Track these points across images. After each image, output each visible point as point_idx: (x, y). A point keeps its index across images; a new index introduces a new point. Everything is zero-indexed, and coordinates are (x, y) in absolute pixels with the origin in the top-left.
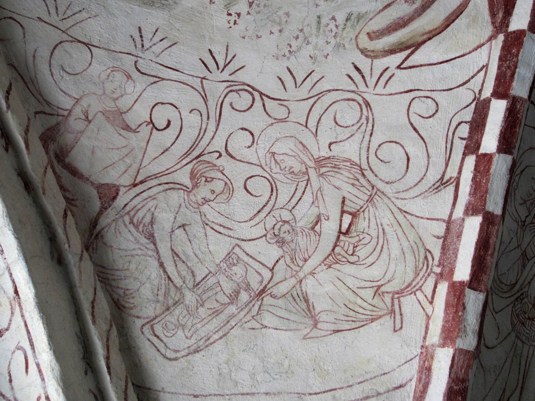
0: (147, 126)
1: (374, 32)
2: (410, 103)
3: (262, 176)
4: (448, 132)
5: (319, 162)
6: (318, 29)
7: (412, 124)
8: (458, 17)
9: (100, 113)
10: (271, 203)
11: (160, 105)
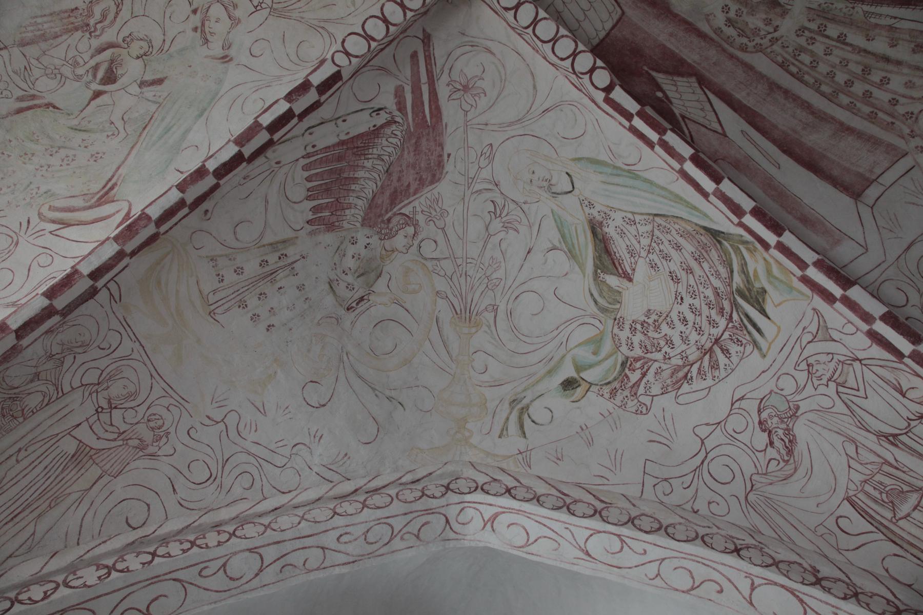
6: (25, 189)
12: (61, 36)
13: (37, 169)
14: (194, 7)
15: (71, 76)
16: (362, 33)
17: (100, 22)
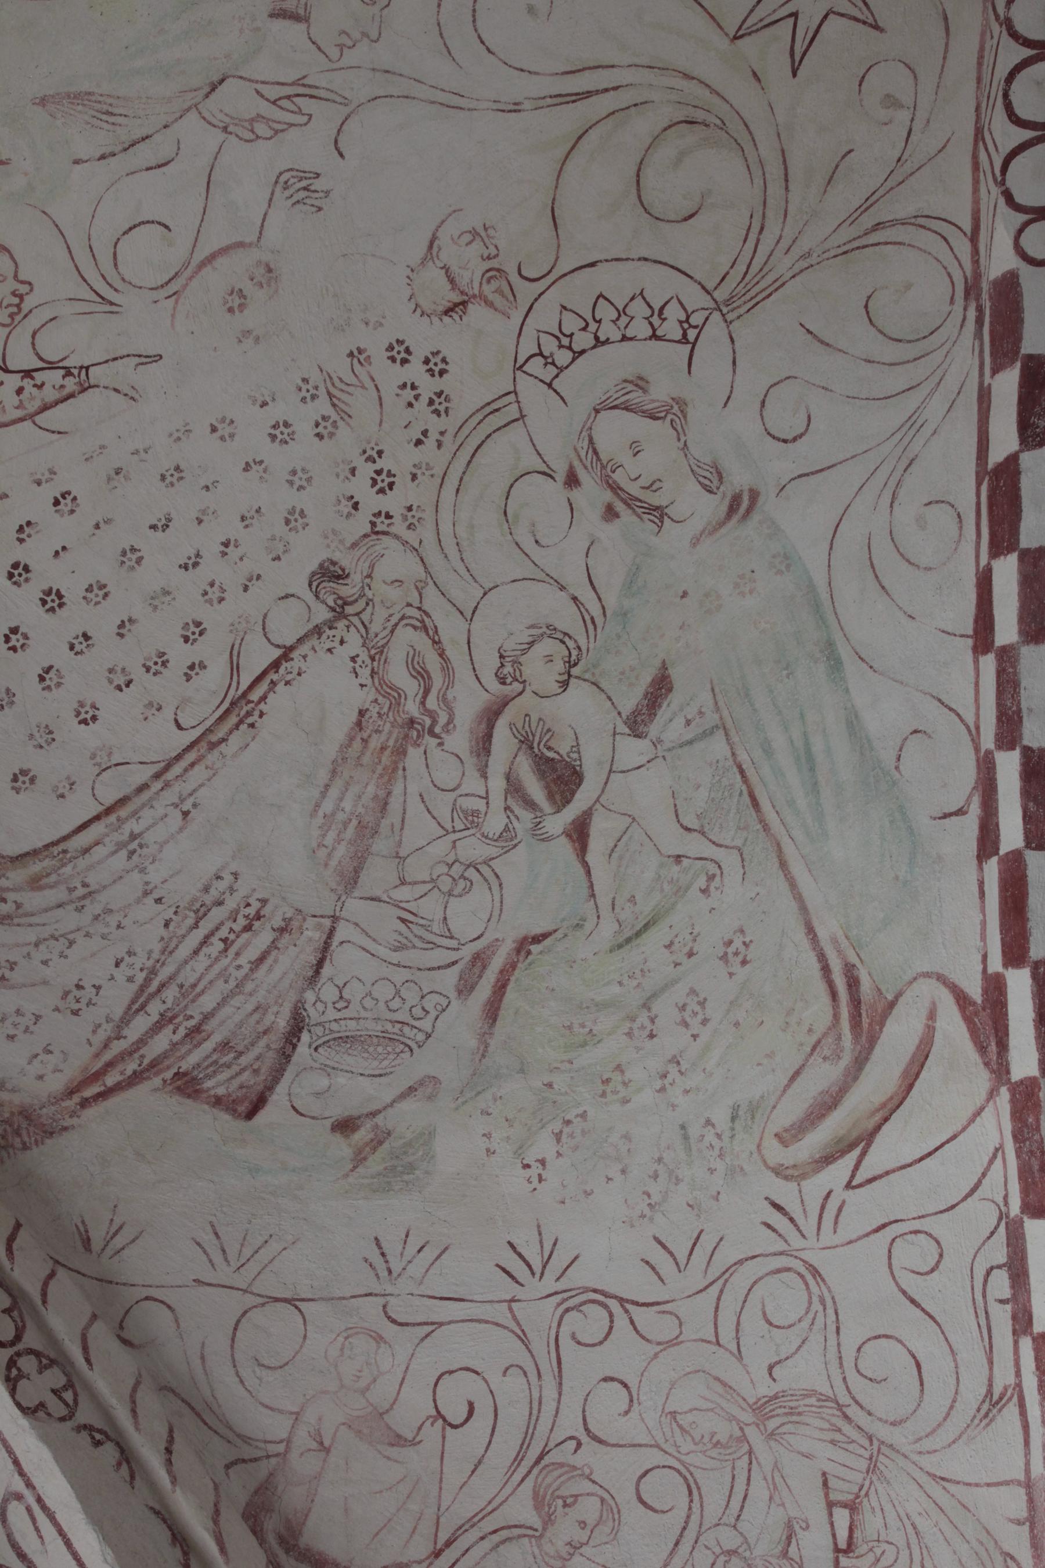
0: (432, 1424)
1: (786, 1131)
2: (890, 1251)
3: (664, 1467)
4: (973, 1294)
5: (762, 1409)
6: (688, 1149)
7: (904, 1293)
8: (922, 1066)
9: (342, 1427)
10: (695, 1518)
11: (446, 1376)
12: (389, 794)
13: (662, 1090)
14: (561, 476)
15: (493, 851)
16: (1029, 134)
17: (427, 692)
